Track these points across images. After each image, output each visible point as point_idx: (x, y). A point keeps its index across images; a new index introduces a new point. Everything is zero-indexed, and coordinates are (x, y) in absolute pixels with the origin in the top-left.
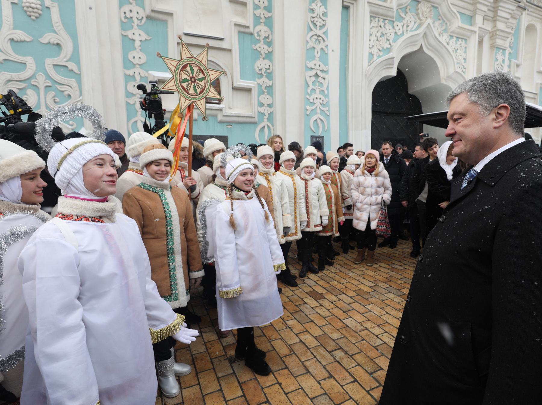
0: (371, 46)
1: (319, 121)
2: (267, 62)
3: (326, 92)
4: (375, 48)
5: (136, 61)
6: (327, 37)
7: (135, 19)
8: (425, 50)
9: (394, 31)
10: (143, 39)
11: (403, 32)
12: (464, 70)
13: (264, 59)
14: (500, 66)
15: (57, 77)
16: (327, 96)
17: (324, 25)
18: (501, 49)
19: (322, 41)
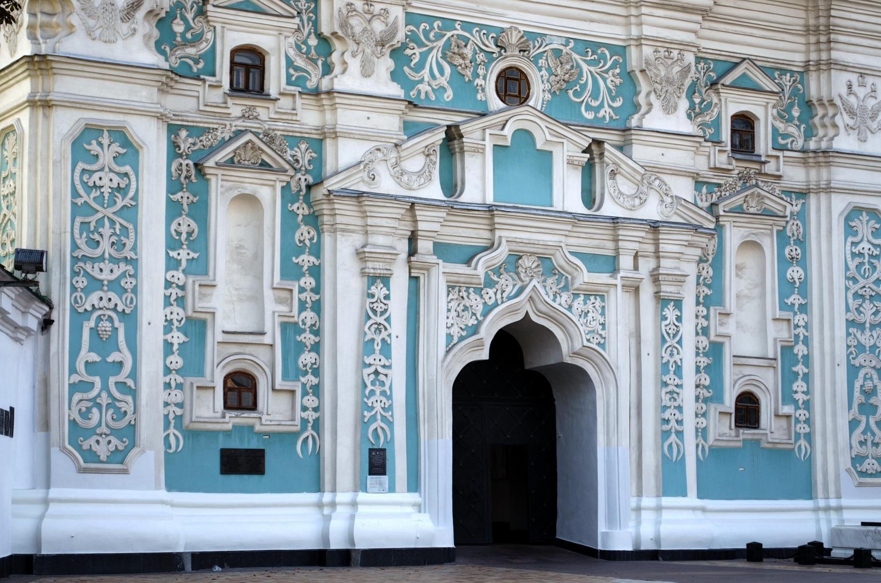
0: (449, 325)
1: (379, 430)
2: (313, 355)
3: (388, 393)
4: (455, 326)
5: (172, 367)
6: (390, 325)
7: (175, 321)
8: (534, 318)
9: (483, 301)
10: (181, 342)
11: (496, 300)
12: (602, 341)
13: (309, 351)
14: (674, 327)
15: (117, 395)
16: (389, 398)
17: (386, 310)
18: (672, 300)
19: (383, 330)
